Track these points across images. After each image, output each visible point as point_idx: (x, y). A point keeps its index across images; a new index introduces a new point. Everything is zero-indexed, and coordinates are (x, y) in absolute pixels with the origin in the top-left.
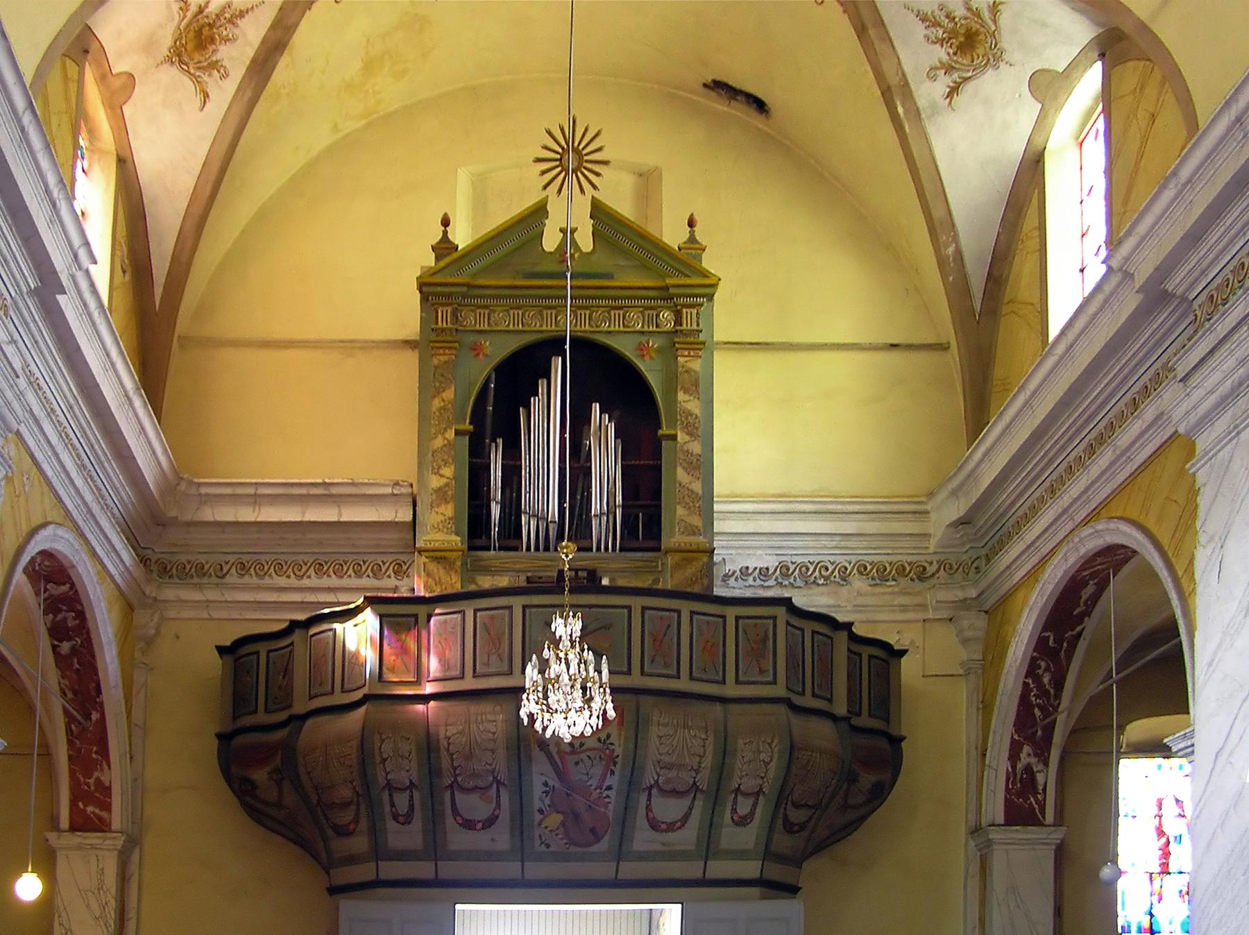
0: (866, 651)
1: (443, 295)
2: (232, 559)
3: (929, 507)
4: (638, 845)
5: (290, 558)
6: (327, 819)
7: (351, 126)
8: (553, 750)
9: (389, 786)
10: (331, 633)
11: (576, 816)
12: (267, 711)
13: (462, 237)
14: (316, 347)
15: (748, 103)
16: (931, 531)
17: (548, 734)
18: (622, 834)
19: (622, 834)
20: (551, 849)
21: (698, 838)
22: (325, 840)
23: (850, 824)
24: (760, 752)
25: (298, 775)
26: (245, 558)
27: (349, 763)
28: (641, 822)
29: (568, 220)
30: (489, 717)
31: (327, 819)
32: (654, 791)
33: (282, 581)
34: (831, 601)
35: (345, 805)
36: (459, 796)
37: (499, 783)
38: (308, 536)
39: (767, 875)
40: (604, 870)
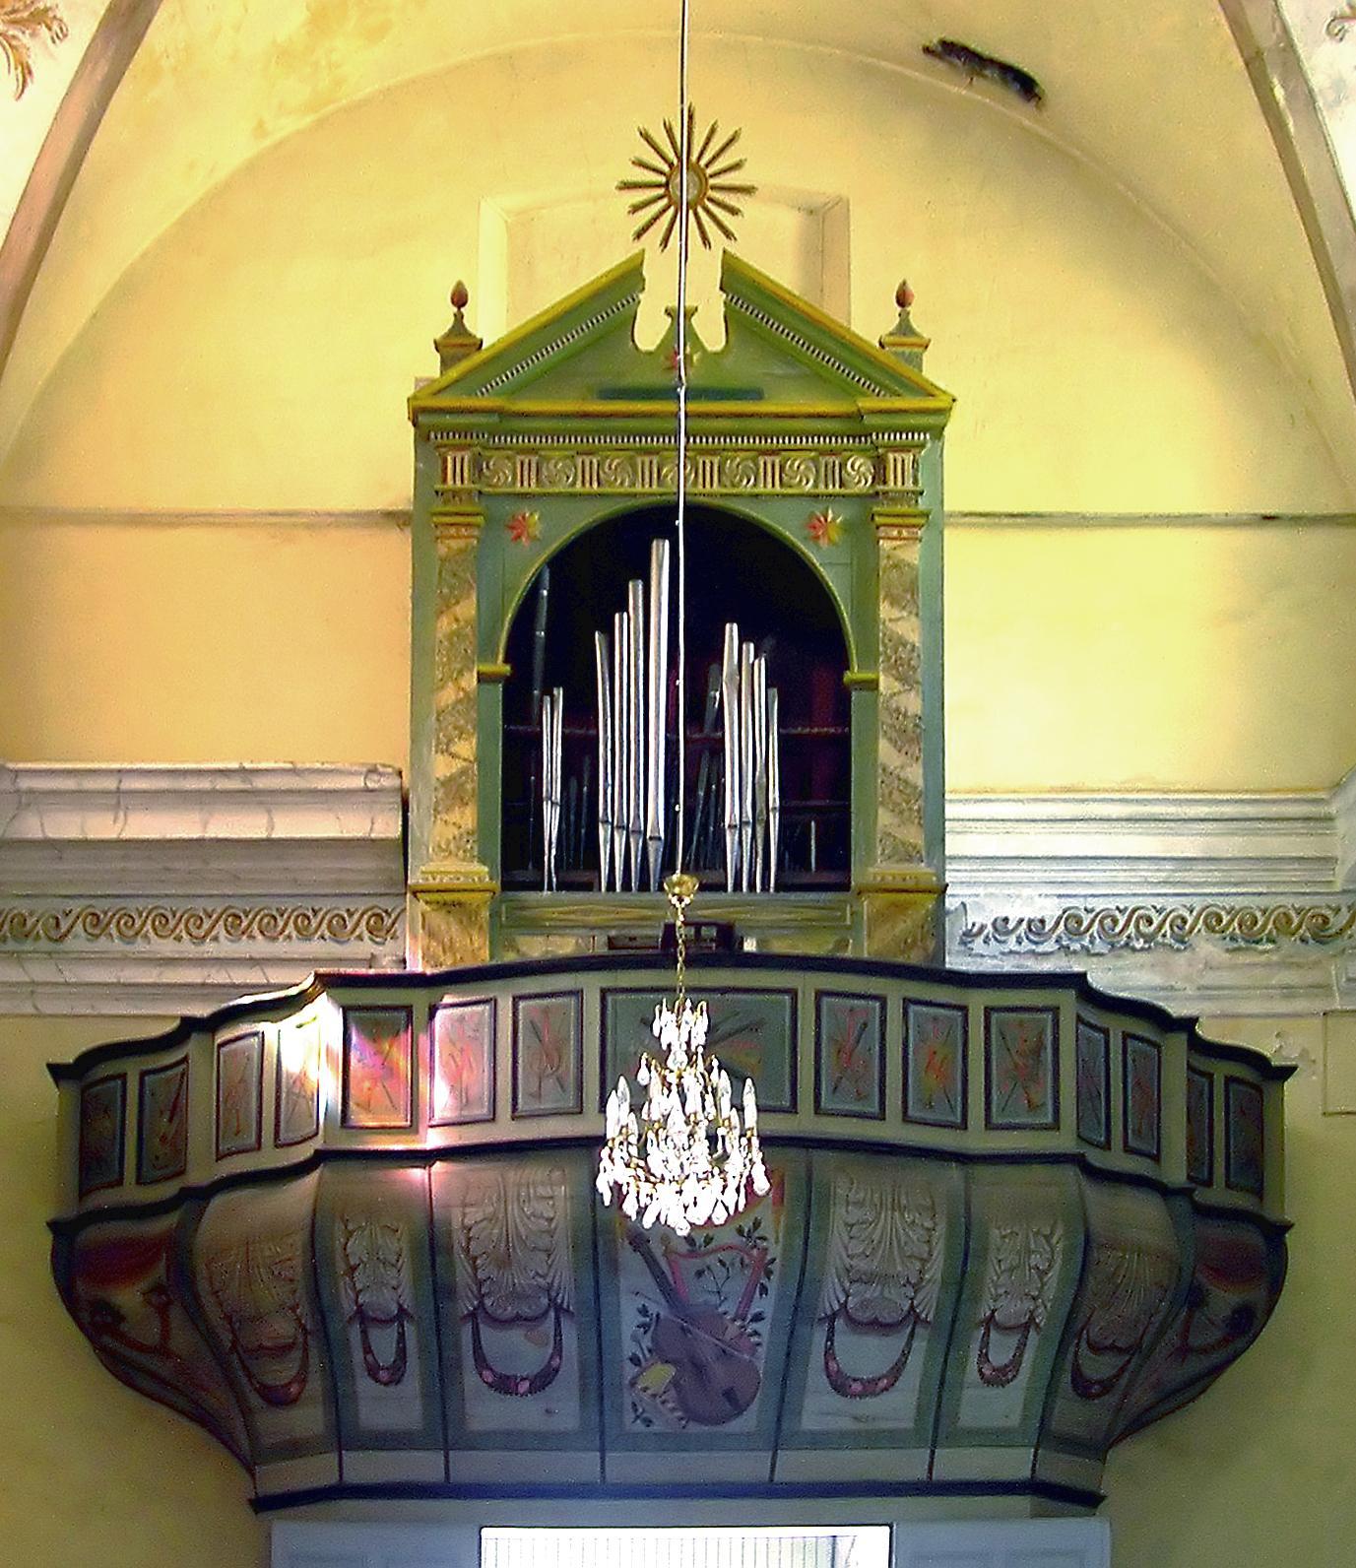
0: (1221, 1070)
1: (455, 430)
2: (77, 906)
3: (1333, 809)
4: (809, 1422)
5: (182, 906)
6: (250, 1376)
7: (286, 127)
8: (657, 1250)
9: (362, 1315)
10: (255, 1041)
11: (699, 1369)
12: (140, 1181)
13: (490, 325)
14: (227, 525)
15: (1004, 81)
16: (1338, 853)
17: (648, 1221)
18: (782, 1400)
19: (782, 1400)
20: (654, 1428)
21: (919, 1407)
22: (246, 1412)
23: (1191, 1383)
24: (1030, 1252)
25: (196, 1297)
26: (100, 906)
27: (289, 1274)
28: (816, 1376)
29: (681, 297)
30: (541, 1191)
31: (250, 1376)
32: (839, 1323)
33: (167, 947)
34: (1157, 980)
35: (283, 1350)
36: (486, 1332)
37: (559, 1309)
38: (214, 865)
39: (1045, 1474)
40: (750, 1466)
